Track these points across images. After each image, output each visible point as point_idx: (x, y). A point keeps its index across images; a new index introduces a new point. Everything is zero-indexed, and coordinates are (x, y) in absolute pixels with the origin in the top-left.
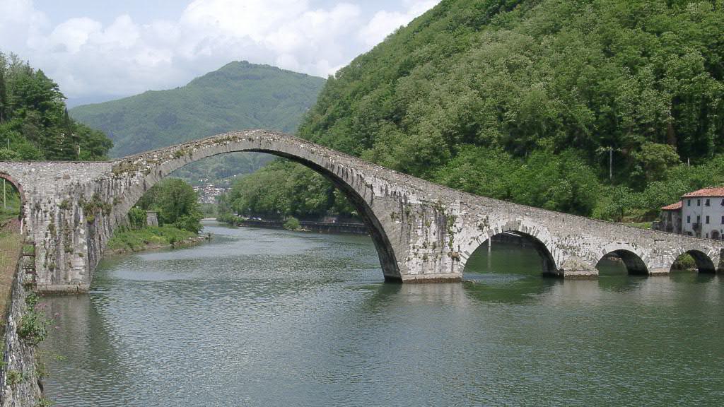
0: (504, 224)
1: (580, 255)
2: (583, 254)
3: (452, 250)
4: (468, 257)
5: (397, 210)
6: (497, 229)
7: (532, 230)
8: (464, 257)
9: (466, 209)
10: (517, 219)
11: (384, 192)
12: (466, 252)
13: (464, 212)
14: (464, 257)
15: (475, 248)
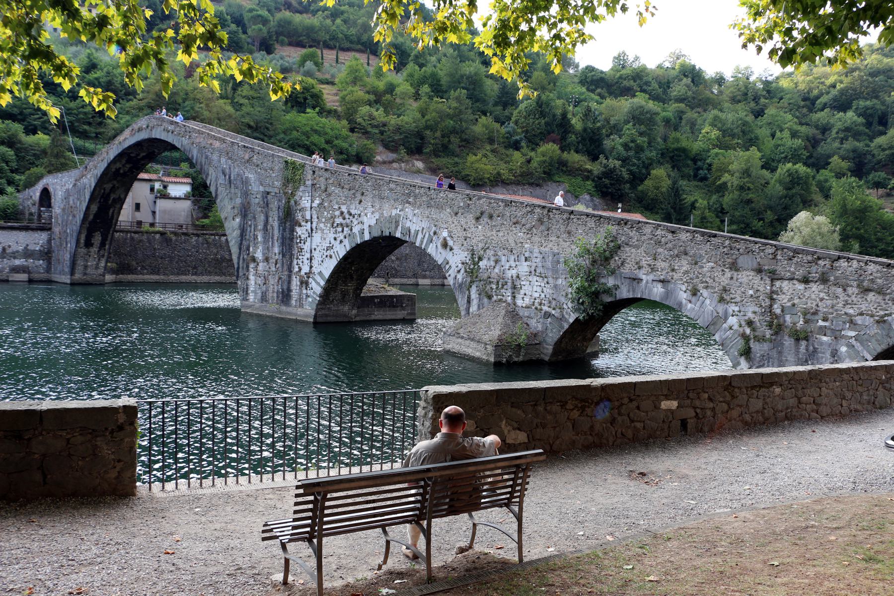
0: (373, 222)
1: (519, 302)
2: (527, 301)
3: (300, 269)
4: (322, 283)
5: (238, 201)
6: (362, 232)
7: (420, 236)
8: (318, 284)
9: (320, 196)
10: (394, 212)
11: (227, 177)
12: (320, 273)
13: (317, 202)
14: (318, 284)
15: (332, 268)
